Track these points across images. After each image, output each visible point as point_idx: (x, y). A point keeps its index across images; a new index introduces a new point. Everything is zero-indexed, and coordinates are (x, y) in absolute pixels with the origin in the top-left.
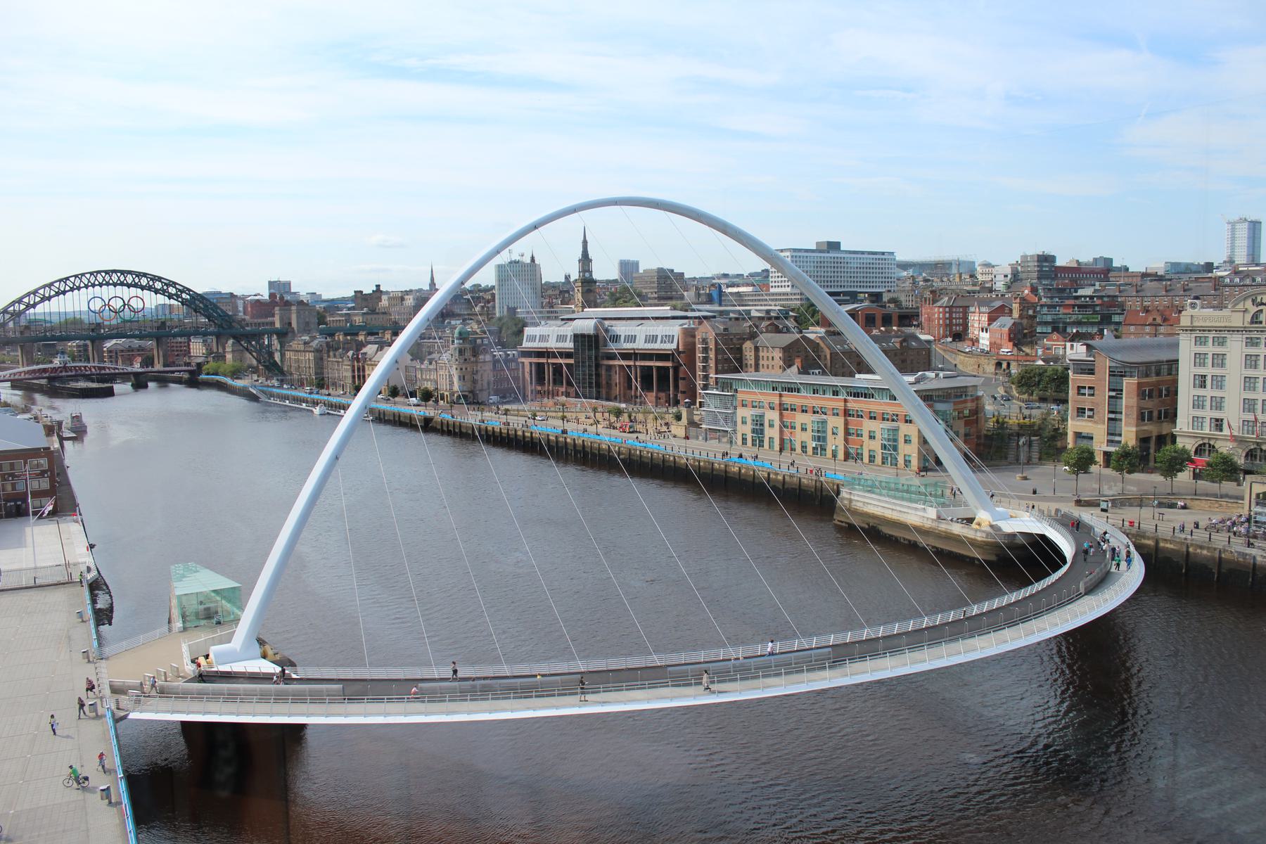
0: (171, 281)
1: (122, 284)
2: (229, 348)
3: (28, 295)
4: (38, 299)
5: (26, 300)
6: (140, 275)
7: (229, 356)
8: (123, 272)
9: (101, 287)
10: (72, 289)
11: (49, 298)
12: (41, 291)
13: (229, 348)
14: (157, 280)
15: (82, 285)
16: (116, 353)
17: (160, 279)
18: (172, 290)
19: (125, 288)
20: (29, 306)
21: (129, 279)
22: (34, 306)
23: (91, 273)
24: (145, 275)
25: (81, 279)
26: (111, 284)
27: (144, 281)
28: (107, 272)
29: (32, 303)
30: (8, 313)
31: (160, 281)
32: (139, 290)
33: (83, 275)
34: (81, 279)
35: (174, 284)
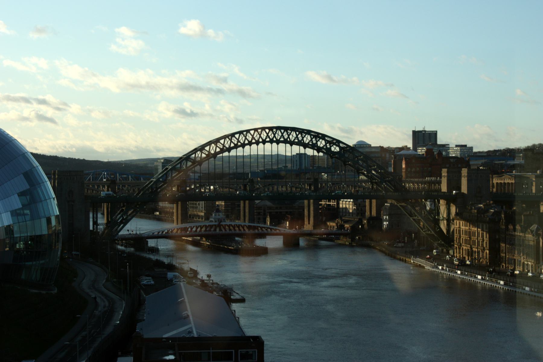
1: (285, 142)
6: (302, 131)
8: (286, 129)
9: (264, 144)
10: (236, 146)
12: (207, 148)
14: (320, 138)
15: (246, 142)
17: (323, 137)
19: (288, 145)
23: (256, 130)
24: (309, 132)
26: (274, 142)
27: (307, 139)
28: (271, 129)
31: (324, 139)
32: (302, 148)
33: (248, 131)
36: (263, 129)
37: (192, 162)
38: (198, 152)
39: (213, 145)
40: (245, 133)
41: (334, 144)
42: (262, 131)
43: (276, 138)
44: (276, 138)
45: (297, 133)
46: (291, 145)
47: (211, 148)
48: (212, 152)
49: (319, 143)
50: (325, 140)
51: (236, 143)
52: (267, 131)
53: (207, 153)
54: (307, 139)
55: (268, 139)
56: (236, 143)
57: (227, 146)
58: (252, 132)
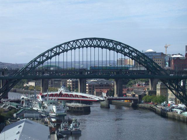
0: (126, 45)
2: (158, 86)
3: (48, 51)
4: (53, 54)
5: (47, 54)
7: (158, 92)
9: (87, 48)
11: (59, 54)
12: (55, 50)
13: (158, 86)
14: (118, 44)
15: (77, 46)
16: (93, 87)
17: (120, 44)
18: (127, 51)
19: (100, 49)
20: (48, 58)
21: (103, 43)
22: (51, 58)
24: (112, 41)
25: (76, 43)
27: (111, 45)
28: (91, 39)
29: (49, 56)
30: (37, 61)
34: (76, 43)
35: (128, 47)
36: (86, 39)
37: (46, 57)
38: (50, 52)
39: (58, 48)
40: (76, 41)
41: (126, 48)
42: (85, 40)
43: (93, 44)
44: (93, 44)
45: (105, 42)
46: (102, 49)
47: (57, 49)
48: (58, 52)
49: (117, 47)
50: (121, 46)
51: (71, 47)
52: (89, 40)
53: (55, 53)
54: (111, 45)
55: (89, 45)
56: (71, 47)
57: (66, 49)
58: (80, 41)
